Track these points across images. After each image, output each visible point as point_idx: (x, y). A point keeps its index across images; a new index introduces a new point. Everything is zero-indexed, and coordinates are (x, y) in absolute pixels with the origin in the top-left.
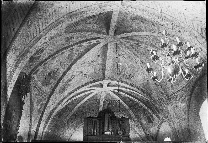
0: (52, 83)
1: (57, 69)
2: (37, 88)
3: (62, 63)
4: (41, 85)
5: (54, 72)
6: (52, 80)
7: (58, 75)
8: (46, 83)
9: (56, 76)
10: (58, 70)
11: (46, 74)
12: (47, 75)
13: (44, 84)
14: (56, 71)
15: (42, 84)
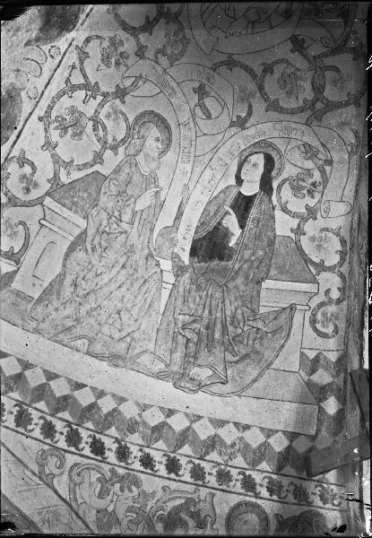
0: (298, 317)
1: (259, 160)
2: (134, 441)
3: (268, 69)
4: (164, 391)
5: (243, 205)
6: (276, 292)
7: (312, 213)
8: (218, 352)
9: (299, 231)
10: (269, 162)
11: (167, 265)
12: (179, 270)
13: (203, 374)
14: (266, 184)
15: (180, 379)
